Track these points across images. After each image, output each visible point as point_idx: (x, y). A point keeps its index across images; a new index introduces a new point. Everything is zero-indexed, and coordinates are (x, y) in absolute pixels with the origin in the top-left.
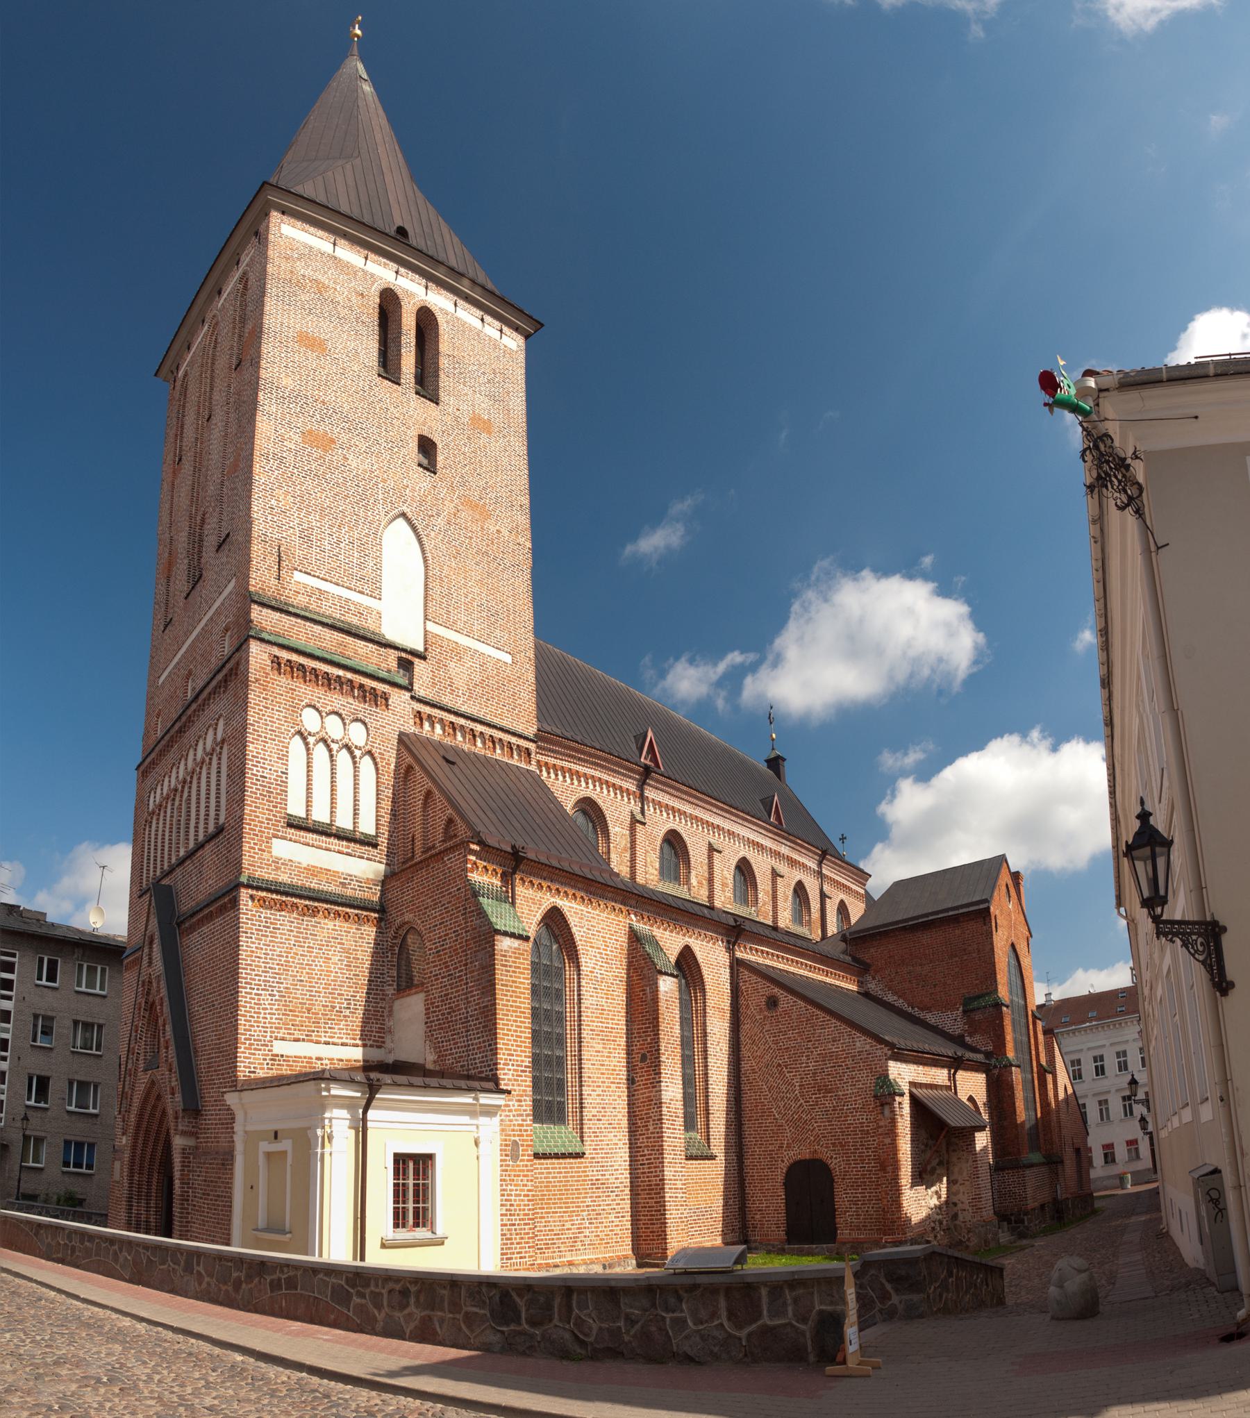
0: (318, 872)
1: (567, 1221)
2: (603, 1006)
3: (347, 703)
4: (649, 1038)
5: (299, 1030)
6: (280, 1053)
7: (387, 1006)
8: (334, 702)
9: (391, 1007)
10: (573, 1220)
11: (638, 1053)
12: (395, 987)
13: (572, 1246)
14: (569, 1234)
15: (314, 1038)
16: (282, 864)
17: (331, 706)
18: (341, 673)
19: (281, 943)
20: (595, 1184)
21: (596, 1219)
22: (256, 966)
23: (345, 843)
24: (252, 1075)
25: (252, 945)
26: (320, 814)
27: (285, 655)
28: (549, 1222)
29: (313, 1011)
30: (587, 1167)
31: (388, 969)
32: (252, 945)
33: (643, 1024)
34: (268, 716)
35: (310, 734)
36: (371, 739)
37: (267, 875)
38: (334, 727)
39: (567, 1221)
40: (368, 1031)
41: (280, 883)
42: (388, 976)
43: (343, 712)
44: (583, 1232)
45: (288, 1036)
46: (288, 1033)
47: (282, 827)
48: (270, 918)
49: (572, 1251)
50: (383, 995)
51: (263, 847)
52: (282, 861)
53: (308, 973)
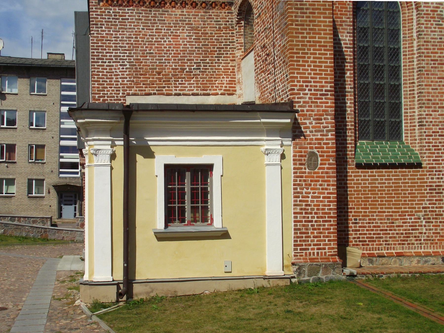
1: (397, 219)
5: (150, 87)
7: (237, 64)
9: (239, 64)
10: (404, 219)
13: (404, 241)
14: (400, 230)
15: (164, 92)
19: (130, 29)
20: (435, 190)
21: (436, 219)
22: (106, 47)
25: (102, 33)
28: (375, 219)
29: (164, 73)
30: (426, 175)
31: (237, 38)
32: (102, 33)
39: (397, 219)
40: (218, 84)
44: (418, 229)
45: (139, 92)
46: (139, 90)
48: (119, 13)
49: (403, 244)
50: (233, 57)
53: (157, 47)
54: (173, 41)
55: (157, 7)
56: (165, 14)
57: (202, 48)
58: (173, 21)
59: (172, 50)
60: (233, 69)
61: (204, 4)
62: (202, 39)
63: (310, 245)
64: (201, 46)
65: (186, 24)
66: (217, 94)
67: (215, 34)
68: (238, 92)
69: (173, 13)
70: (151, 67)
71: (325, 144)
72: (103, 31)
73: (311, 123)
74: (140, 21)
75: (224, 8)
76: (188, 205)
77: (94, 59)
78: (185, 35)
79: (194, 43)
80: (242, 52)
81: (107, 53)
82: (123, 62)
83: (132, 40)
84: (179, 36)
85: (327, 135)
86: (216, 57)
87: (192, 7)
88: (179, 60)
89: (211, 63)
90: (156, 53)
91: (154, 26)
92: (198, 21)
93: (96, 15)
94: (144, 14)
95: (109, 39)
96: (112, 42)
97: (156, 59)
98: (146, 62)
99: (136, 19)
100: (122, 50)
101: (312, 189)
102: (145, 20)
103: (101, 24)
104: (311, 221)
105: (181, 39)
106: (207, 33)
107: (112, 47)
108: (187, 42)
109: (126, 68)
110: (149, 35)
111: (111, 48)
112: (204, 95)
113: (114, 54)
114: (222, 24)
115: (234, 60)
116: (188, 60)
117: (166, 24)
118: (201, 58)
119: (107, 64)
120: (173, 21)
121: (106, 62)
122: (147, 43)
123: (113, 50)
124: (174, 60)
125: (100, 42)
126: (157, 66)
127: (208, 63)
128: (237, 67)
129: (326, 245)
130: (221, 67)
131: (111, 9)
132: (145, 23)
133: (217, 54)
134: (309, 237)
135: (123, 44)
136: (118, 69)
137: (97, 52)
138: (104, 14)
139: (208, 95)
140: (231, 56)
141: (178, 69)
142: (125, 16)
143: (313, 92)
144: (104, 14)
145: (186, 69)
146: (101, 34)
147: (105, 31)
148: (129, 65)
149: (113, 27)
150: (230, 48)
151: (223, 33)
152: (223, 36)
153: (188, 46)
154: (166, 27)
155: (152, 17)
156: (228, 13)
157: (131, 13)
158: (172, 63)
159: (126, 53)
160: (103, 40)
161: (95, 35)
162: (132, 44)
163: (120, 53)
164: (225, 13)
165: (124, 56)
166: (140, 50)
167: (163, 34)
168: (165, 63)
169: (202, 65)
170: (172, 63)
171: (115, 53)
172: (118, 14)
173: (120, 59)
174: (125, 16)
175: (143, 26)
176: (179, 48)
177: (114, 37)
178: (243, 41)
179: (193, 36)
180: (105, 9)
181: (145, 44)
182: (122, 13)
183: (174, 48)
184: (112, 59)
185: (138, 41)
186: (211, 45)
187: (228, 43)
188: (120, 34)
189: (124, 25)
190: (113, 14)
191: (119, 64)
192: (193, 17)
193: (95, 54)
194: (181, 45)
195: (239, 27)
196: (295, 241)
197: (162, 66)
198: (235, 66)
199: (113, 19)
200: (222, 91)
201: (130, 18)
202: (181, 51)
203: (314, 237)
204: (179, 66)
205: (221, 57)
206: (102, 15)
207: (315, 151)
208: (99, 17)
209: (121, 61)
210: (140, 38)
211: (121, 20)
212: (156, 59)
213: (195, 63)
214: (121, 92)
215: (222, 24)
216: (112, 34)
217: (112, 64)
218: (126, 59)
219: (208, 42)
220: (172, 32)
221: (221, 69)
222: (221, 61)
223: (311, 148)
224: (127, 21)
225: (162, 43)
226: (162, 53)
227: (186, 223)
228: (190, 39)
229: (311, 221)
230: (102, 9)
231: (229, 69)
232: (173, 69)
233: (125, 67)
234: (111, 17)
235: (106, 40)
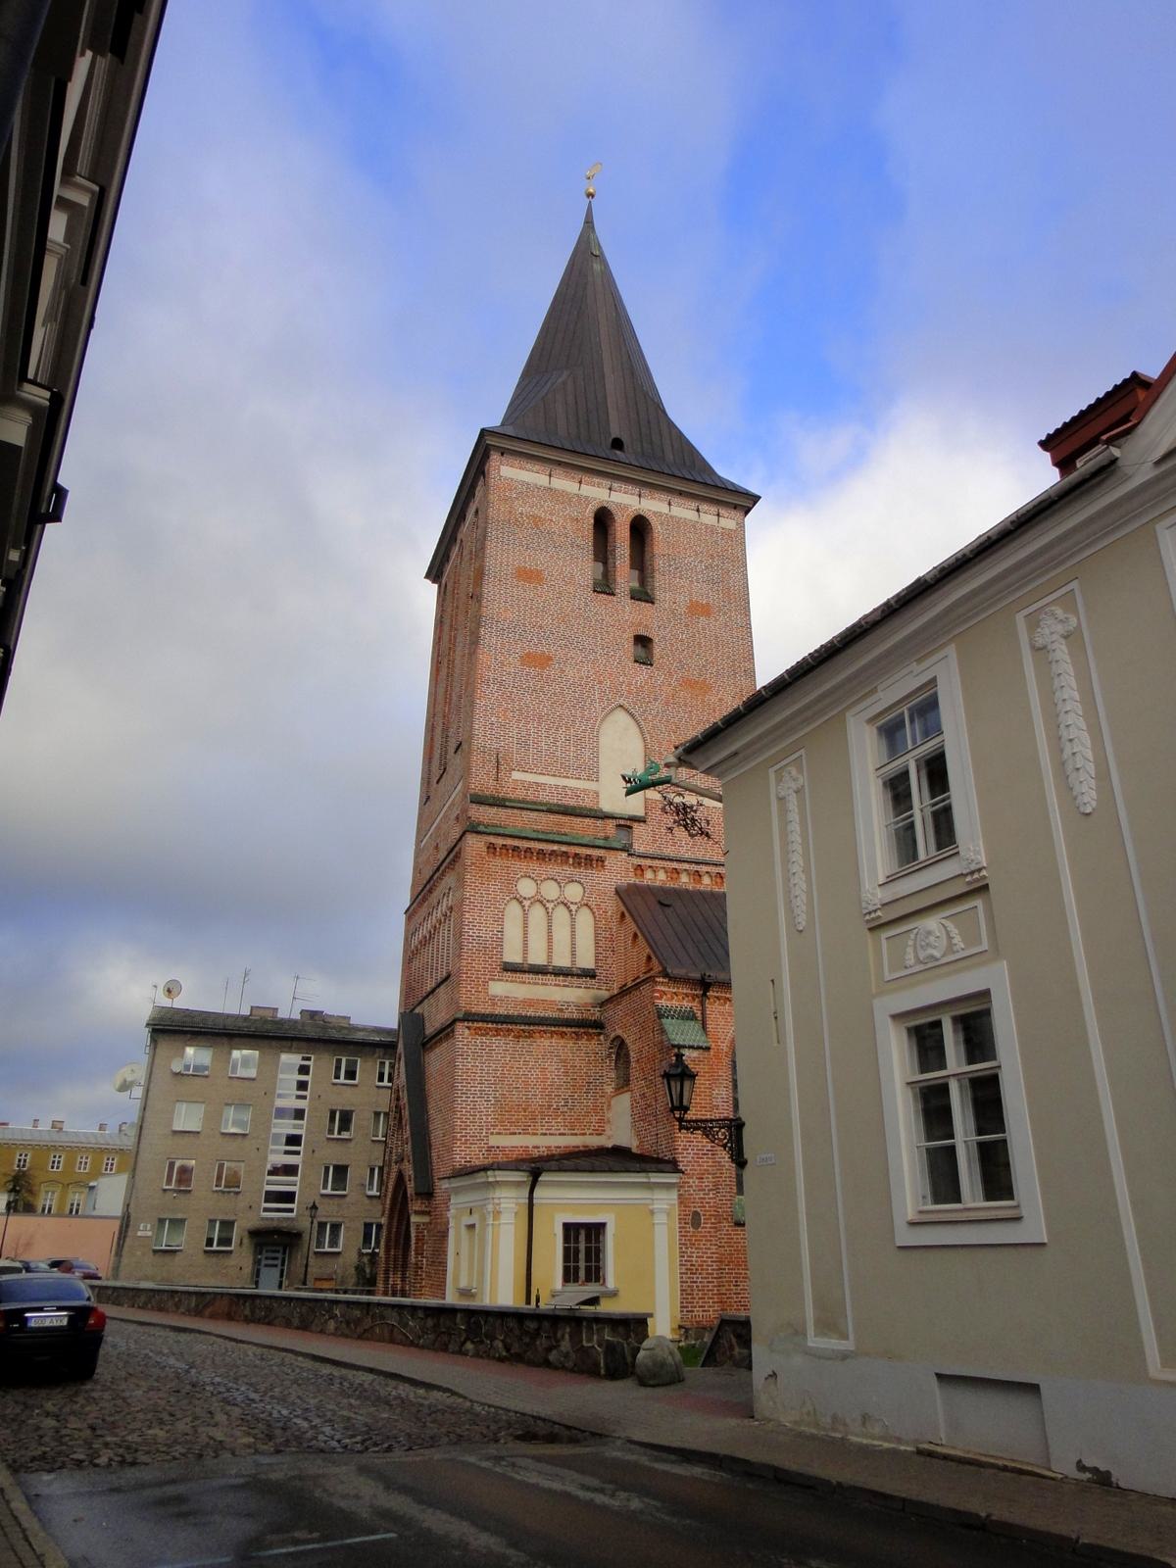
6: (496, 1145)
9: (609, 1102)
18: (555, 847)
23: (561, 978)
24: (468, 1164)
26: (537, 958)
27: (500, 841)
35: (525, 898)
38: (550, 890)
63: (695, 1307)
66: (585, 1134)
68: (608, 1132)
71: (707, 1203)
73: (694, 1182)
76: (582, 1264)
85: (708, 1194)
101: (696, 1249)
104: (696, 1282)
112: (572, 1134)
116: (556, 1095)
129: (710, 1307)
134: (694, 1298)
136: (482, 1105)
139: (576, 1134)
143: (695, 1151)
196: (682, 1303)
200: (591, 1131)
203: (699, 1299)
207: (698, 1210)
214: (485, 1131)
223: (695, 1207)
227: (580, 1283)
229: (696, 1282)
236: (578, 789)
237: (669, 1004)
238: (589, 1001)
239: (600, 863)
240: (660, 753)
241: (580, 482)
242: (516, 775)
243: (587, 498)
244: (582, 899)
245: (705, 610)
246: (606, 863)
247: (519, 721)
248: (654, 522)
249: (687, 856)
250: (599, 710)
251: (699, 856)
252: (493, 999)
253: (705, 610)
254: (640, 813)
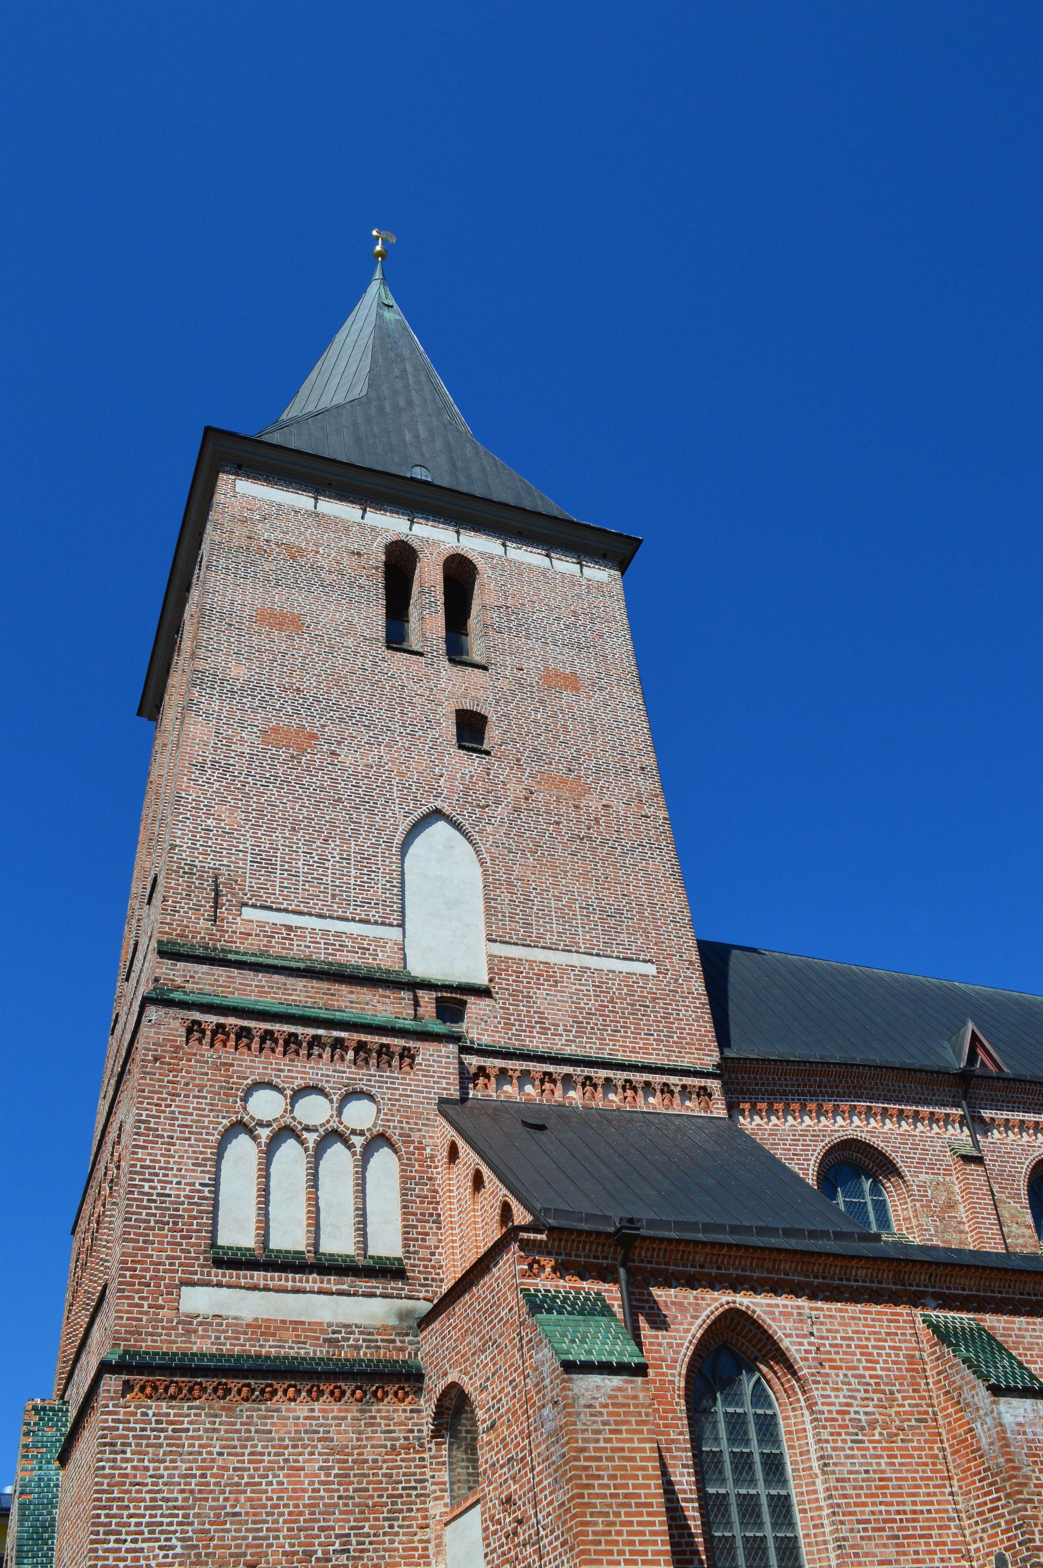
0: (277, 1328)
2: (883, 1472)
3: (334, 1071)
4: (1002, 1522)
8: (308, 1073)
11: (988, 1555)
12: (447, 1500)
16: (200, 1324)
17: (302, 1078)
19: (190, 1454)
25: (124, 1465)
32: (124, 1465)
33: (986, 1494)
34: (177, 1106)
36: (382, 1116)
37: (165, 1346)
41: (194, 1355)
42: (433, 1484)
43: (326, 1085)
47: (201, 1266)
51: (161, 1302)
52: (199, 1319)
53: (250, 1499)
54: (289, 1483)
55: (254, 1401)
56: (272, 1417)
57: (352, 1498)
58: (289, 1432)
59: (286, 1506)
60: (425, 1549)
61: (358, 1391)
62: (355, 1476)
64: (351, 1494)
65: (320, 1440)
67: (384, 1461)
69: (291, 1415)
70: (233, 1550)
72: (127, 1460)
74: (215, 1435)
75: (402, 1401)
77: (97, 1533)
78: (317, 1465)
79: (336, 1486)
80: (446, 1505)
81: (131, 1516)
82: (167, 1540)
83: (193, 1481)
84: (303, 1469)
86: (386, 1519)
87: (332, 1399)
88: (300, 1529)
89: (375, 1535)
90: (247, 1514)
91: (245, 1447)
92: (346, 1432)
93: (113, 1421)
94: (224, 1419)
95: (138, 1480)
96: (145, 1489)
97: (247, 1530)
98: (222, 1539)
99: (206, 1430)
100: (168, 1508)
102: (226, 1431)
103: (123, 1444)
105: (306, 1476)
106: (366, 1461)
107: (144, 1500)
108: (321, 1483)
109: (175, 1556)
110: (235, 1469)
111: (142, 1504)
113: (147, 1519)
114: (398, 1439)
115: (427, 1526)
116: (322, 1529)
117: (273, 1439)
118: (352, 1524)
119: (128, 1545)
120: (289, 1432)
121: (125, 1541)
122: (228, 1489)
123: (146, 1508)
124: (290, 1529)
125: (116, 1489)
126: (248, 1546)
127: (368, 1535)
128: (433, 1542)
130: (396, 1545)
131: (150, 1407)
132: (227, 1439)
133: (389, 1512)
135: (171, 1491)
137: (107, 1516)
138: (132, 1419)
140: (419, 1515)
141: (296, 1553)
142: (182, 1423)
144: (132, 1419)
145: (316, 1552)
146: (121, 1468)
147: (132, 1460)
148: (182, 1547)
149: (150, 1450)
150: (417, 1496)
151: (402, 1460)
152: (400, 1467)
153: (322, 1493)
154: (273, 1447)
155: (242, 1424)
156: (412, 1411)
157: (195, 1415)
158: (284, 1538)
159: (177, 1516)
160: (124, 1484)
161: (107, 1471)
162: (192, 1491)
163: (162, 1515)
164: (404, 1411)
165: (171, 1524)
166: (211, 1508)
167: (266, 1464)
168: (267, 1538)
169: (354, 1540)
170: (284, 1538)
171: (151, 1516)
172: (164, 1419)
173: (162, 1532)
174: (182, 1423)
175: (222, 1447)
176: (301, 1498)
177: (151, 1476)
178: (447, 1479)
179: (333, 1468)
180: (137, 1407)
181: (223, 1492)
182: (175, 1415)
183: (290, 1498)
184: (142, 1533)
185: (208, 1484)
186: (374, 1490)
187: (413, 1484)
188: (166, 1468)
189: (177, 1446)
190: (154, 1419)
191: (157, 1544)
192: (334, 1422)
193: (103, 1519)
194: (304, 1490)
195: (437, 1444)
197: (261, 1546)
198: (428, 1541)
199: (153, 1430)
201: (191, 1427)
202: (305, 1506)
204: (300, 1545)
205: (397, 1519)
206: (129, 1422)
208: (121, 1426)
209: (163, 1537)
210: (213, 1476)
211: (170, 1433)
212: (247, 1530)
213: (337, 1536)
215: (398, 1439)
216: (147, 1469)
217: (139, 1545)
218: (176, 1532)
219: (368, 1483)
220: (286, 1461)
221: (397, 1550)
222: (396, 1529)
224: (184, 1435)
225: (264, 1487)
226: (260, 1514)
228: (328, 1475)
230: (129, 1407)
231: (416, 1549)
232: (285, 1554)
233: (171, 1553)
234: (149, 1427)
235: (131, 1484)
236: (364, 938)
237: (550, 1285)
238: (393, 1322)
239: (407, 1061)
240: (510, 883)
241: (365, 511)
242: (248, 913)
243: (373, 529)
244: (375, 1125)
245: (572, 682)
246: (418, 1059)
247: (256, 826)
248: (480, 564)
249: (568, 1051)
250: (400, 816)
251: (592, 1052)
252: (189, 1323)
253: (572, 682)
254: (482, 979)
